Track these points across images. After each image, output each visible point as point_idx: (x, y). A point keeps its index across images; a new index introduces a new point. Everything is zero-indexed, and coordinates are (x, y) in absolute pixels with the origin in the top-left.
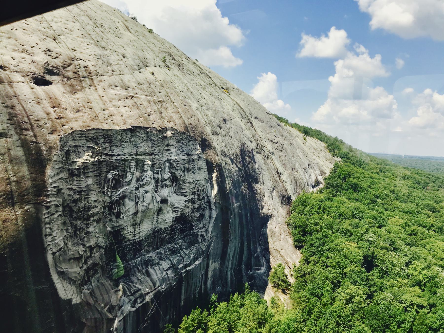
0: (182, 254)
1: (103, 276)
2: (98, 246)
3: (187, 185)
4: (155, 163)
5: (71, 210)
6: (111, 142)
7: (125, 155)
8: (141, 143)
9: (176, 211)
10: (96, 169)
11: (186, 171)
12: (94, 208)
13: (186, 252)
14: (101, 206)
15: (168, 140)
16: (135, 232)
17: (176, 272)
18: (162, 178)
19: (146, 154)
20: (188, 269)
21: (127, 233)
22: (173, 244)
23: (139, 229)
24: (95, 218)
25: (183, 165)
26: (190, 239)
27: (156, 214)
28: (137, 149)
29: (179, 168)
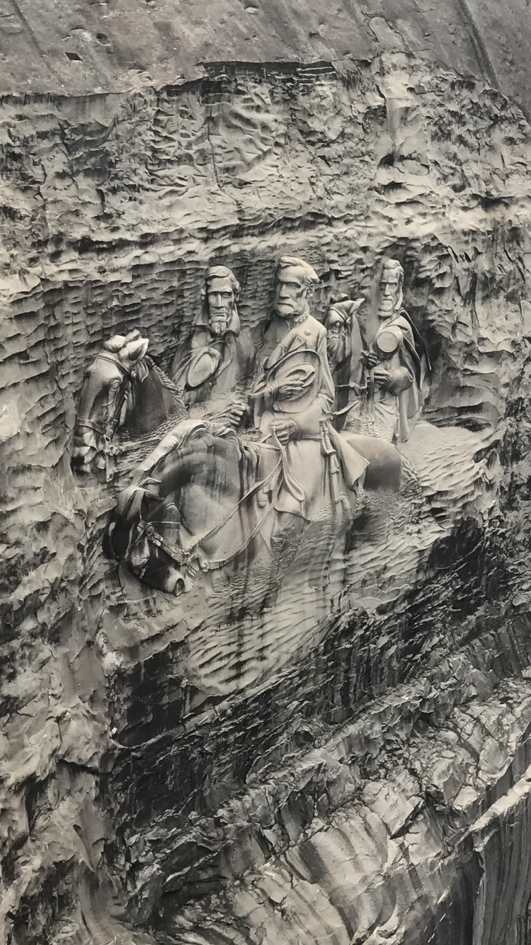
0: (469, 728)
1: (97, 919)
2: (68, 767)
3: (485, 368)
4: (335, 266)
6: (103, 169)
7: (180, 237)
8: (259, 158)
9: (434, 511)
10: (33, 342)
11: (479, 295)
12: (35, 566)
13: (484, 720)
14: (71, 550)
16: (239, 654)
17: (445, 834)
18: (366, 348)
19: (287, 224)
20: (502, 806)
21: (202, 666)
22: (421, 685)
23: (262, 636)
24: (42, 616)
25: (466, 265)
26: (498, 646)
27: (340, 543)
28: (238, 194)
29: (447, 283)
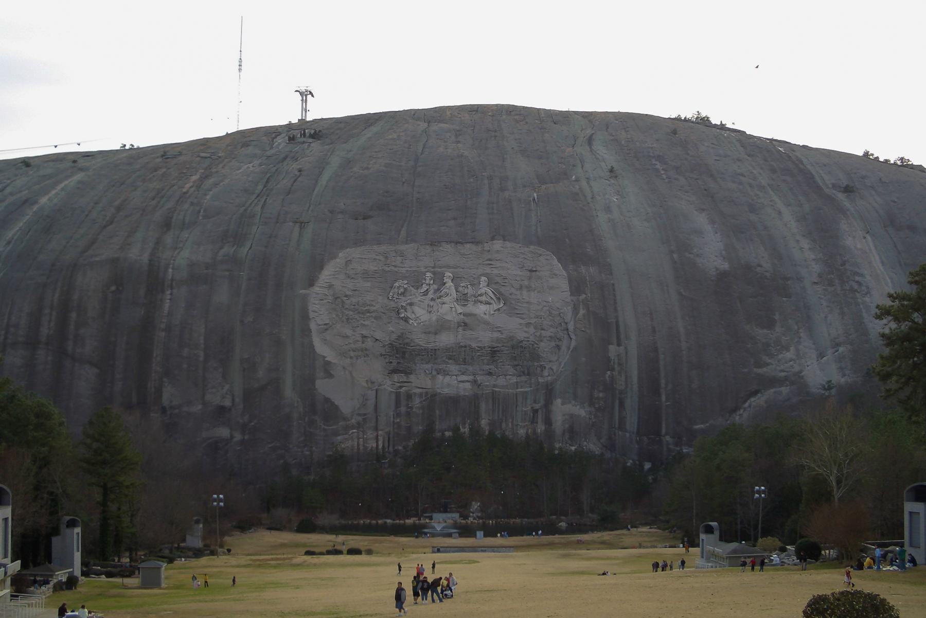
3: (525, 305)
5: (343, 302)
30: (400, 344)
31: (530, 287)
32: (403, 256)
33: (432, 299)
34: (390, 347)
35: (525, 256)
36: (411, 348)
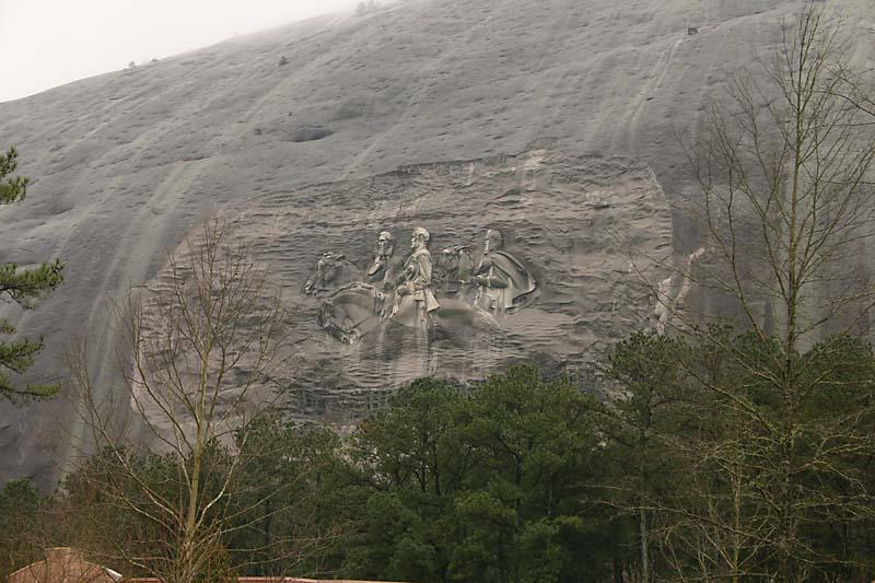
15: (519, 181)
30: (317, 384)
31: (592, 243)
32: (341, 204)
33: (387, 288)
34: (294, 392)
35: (591, 177)
36: (334, 392)
